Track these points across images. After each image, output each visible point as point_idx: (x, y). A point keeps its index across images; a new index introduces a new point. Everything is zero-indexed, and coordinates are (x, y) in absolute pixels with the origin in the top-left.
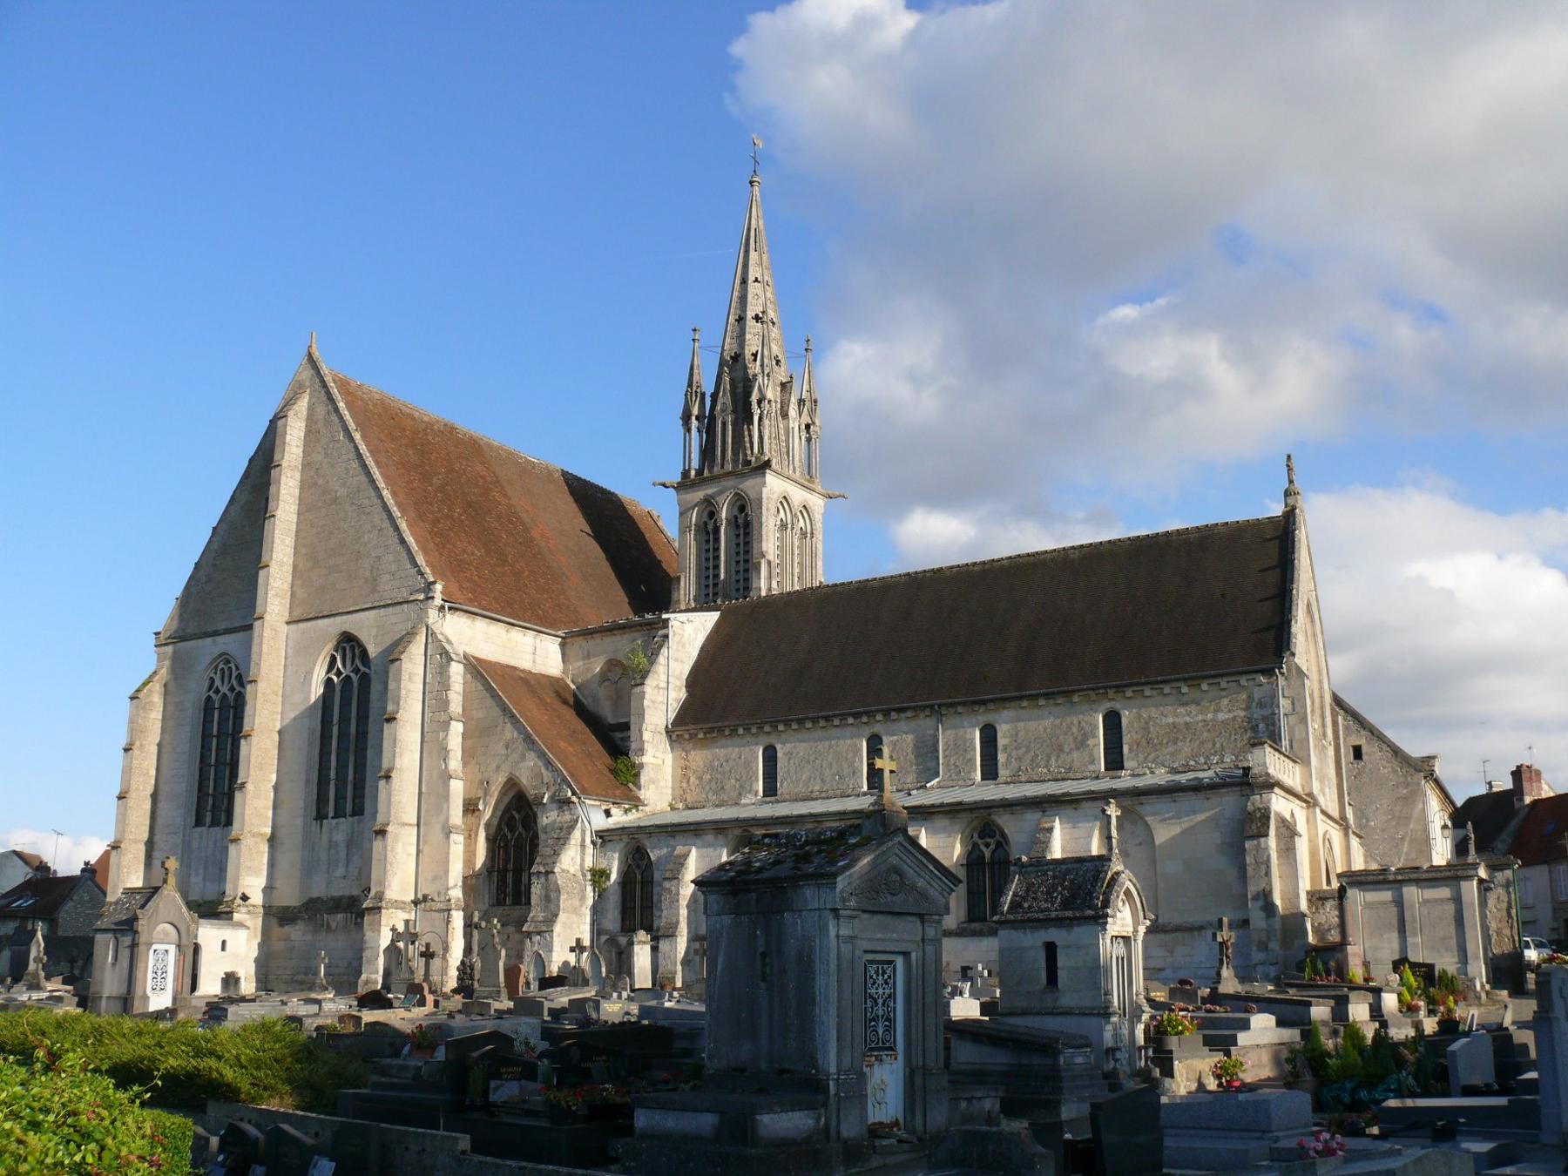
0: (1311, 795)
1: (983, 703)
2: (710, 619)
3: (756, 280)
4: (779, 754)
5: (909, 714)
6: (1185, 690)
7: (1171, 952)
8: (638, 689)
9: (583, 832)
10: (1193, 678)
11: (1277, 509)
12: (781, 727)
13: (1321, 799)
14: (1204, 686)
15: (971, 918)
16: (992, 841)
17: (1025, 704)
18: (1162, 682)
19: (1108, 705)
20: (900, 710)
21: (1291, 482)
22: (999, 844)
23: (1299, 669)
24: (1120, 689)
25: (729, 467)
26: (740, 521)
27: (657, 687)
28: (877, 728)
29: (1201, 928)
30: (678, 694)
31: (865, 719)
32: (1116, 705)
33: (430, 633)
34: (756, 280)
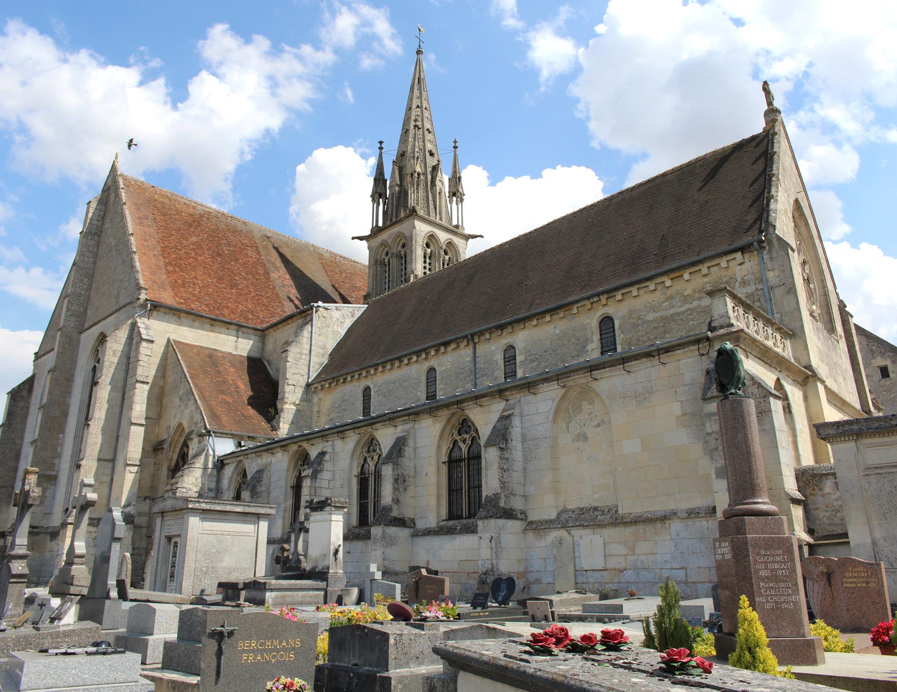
0: (809, 367)
1: (502, 327)
2: (359, 309)
3: (418, 107)
4: (372, 393)
5: (453, 346)
6: (668, 283)
7: (632, 549)
8: (284, 355)
9: (207, 456)
10: (673, 270)
11: (758, 126)
12: (372, 372)
13: (822, 370)
14: (686, 276)
15: (451, 517)
16: (467, 436)
17: (535, 322)
18: (648, 279)
19: (600, 312)
20: (446, 344)
21: (770, 103)
22: (473, 439)
23: (779, 239)
24: (610, 292)
25: (394, 220)
26: (403, 253)
27: (301, 354)
28: (433, 362)
29: (664, 518)
30: (320, 360)
31: (424, 356)
32: (610, 310)
33: (134, 325)
34: (418, 107)
